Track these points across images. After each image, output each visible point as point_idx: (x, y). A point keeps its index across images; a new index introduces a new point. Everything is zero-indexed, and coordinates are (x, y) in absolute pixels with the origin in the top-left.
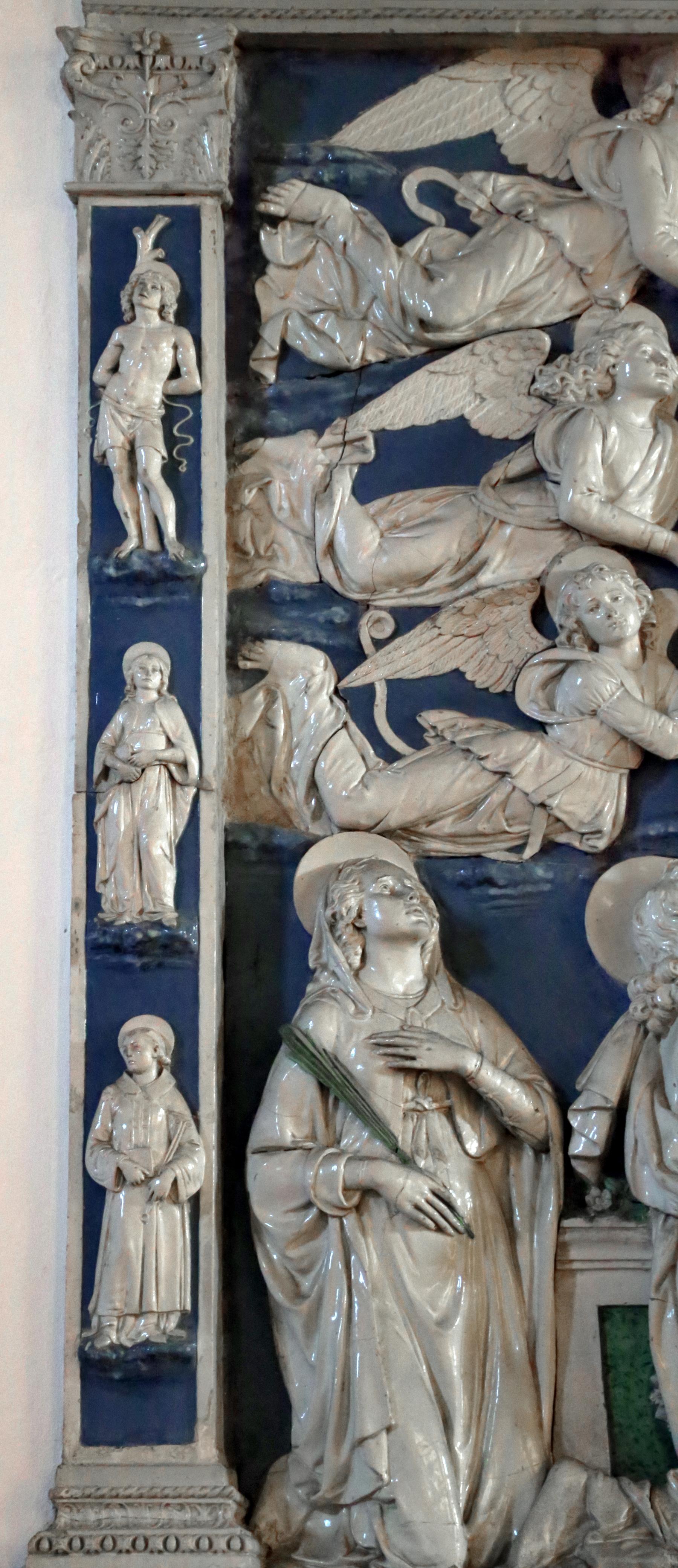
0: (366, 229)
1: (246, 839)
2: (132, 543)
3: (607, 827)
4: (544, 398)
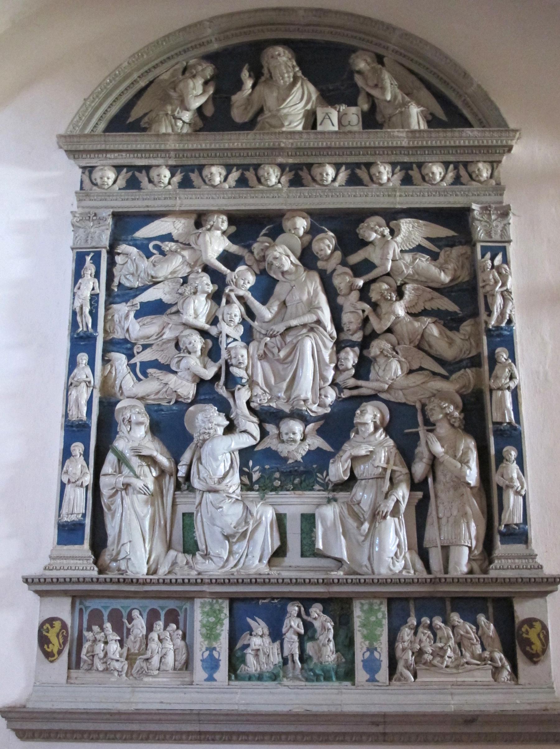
0: (140, 255)
1: (104, 400)
2: (81, 329)
3: (191, 396)
4: (181, 294)
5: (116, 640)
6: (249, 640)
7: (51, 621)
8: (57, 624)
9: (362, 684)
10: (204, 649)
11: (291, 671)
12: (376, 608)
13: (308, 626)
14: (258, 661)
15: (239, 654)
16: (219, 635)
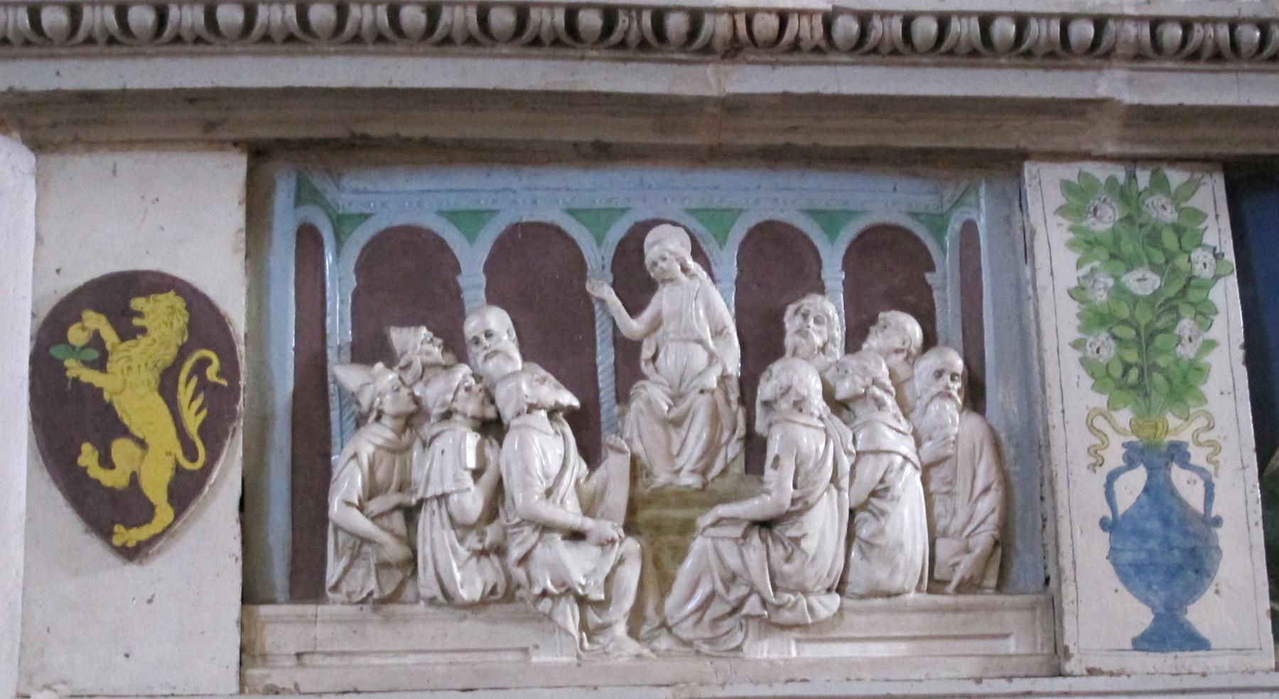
5: (552, 413)
7: (117, 296)
8: (162, 319)
10: (1114, 457)
16: (1197, 370)
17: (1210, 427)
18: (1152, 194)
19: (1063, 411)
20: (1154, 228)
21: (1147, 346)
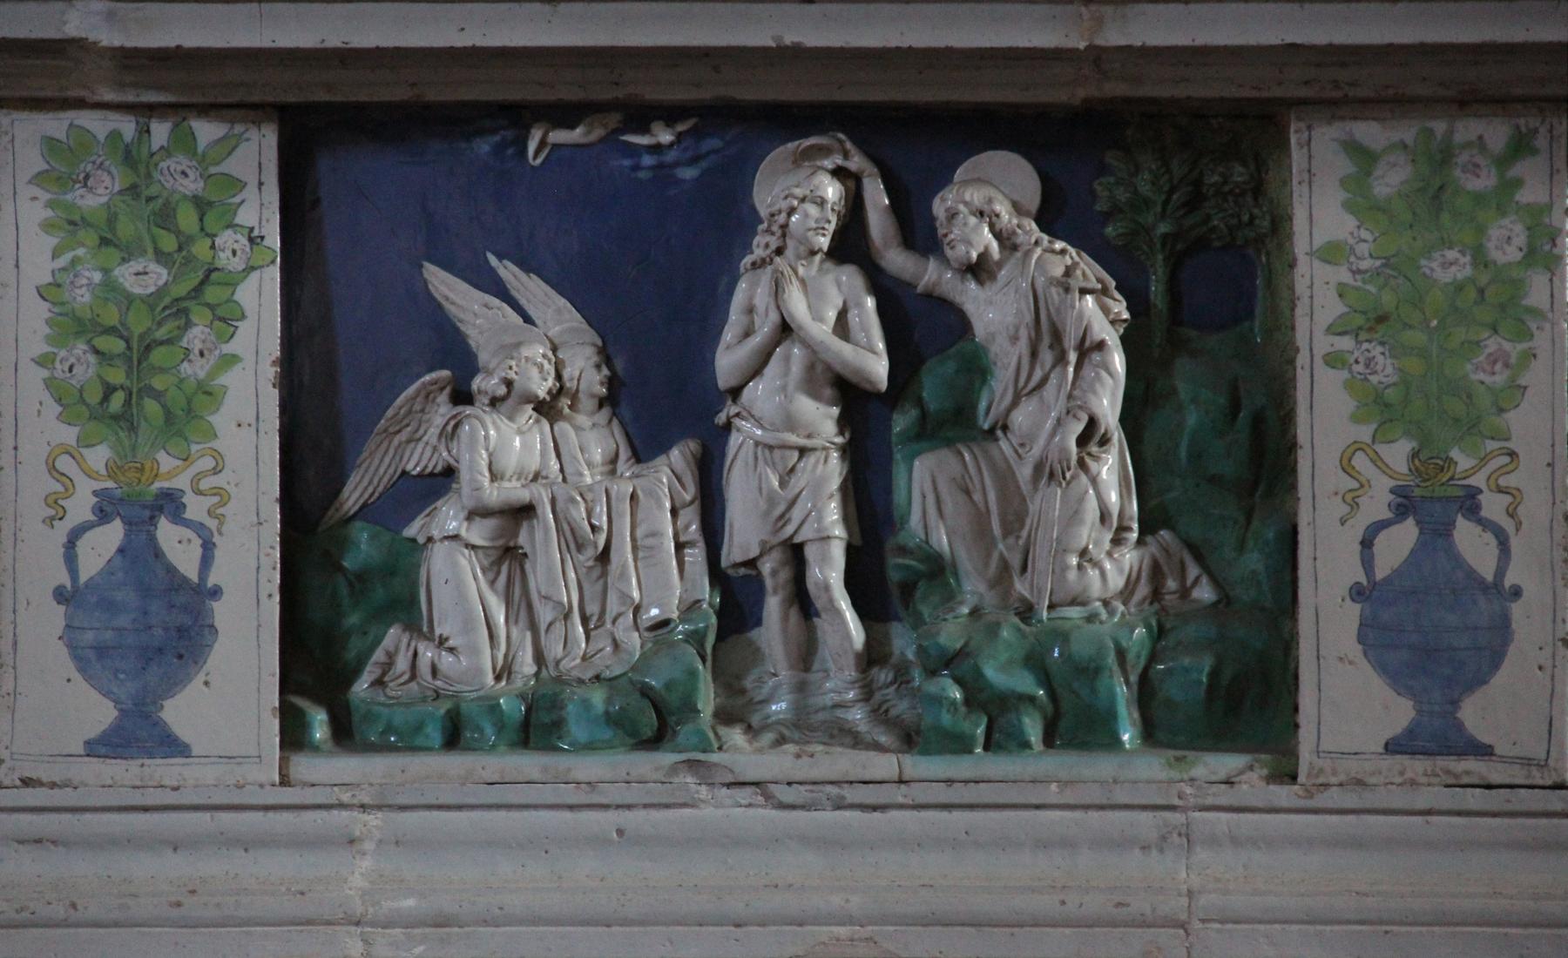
6: (451, 433)
9: (1353, 767)
10: (81, 507)
11: (785, 674)
12: (1484, 181)
13: (921, 328)
14: (520, 603)
15: (364, 546)
16: (209, 393)
17: (216, 471)
18: (169, 155)
19: (16, 448)
20: (167, 204)
21: (139, 363)
